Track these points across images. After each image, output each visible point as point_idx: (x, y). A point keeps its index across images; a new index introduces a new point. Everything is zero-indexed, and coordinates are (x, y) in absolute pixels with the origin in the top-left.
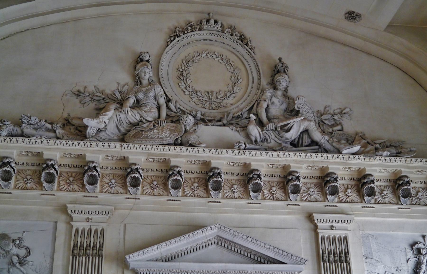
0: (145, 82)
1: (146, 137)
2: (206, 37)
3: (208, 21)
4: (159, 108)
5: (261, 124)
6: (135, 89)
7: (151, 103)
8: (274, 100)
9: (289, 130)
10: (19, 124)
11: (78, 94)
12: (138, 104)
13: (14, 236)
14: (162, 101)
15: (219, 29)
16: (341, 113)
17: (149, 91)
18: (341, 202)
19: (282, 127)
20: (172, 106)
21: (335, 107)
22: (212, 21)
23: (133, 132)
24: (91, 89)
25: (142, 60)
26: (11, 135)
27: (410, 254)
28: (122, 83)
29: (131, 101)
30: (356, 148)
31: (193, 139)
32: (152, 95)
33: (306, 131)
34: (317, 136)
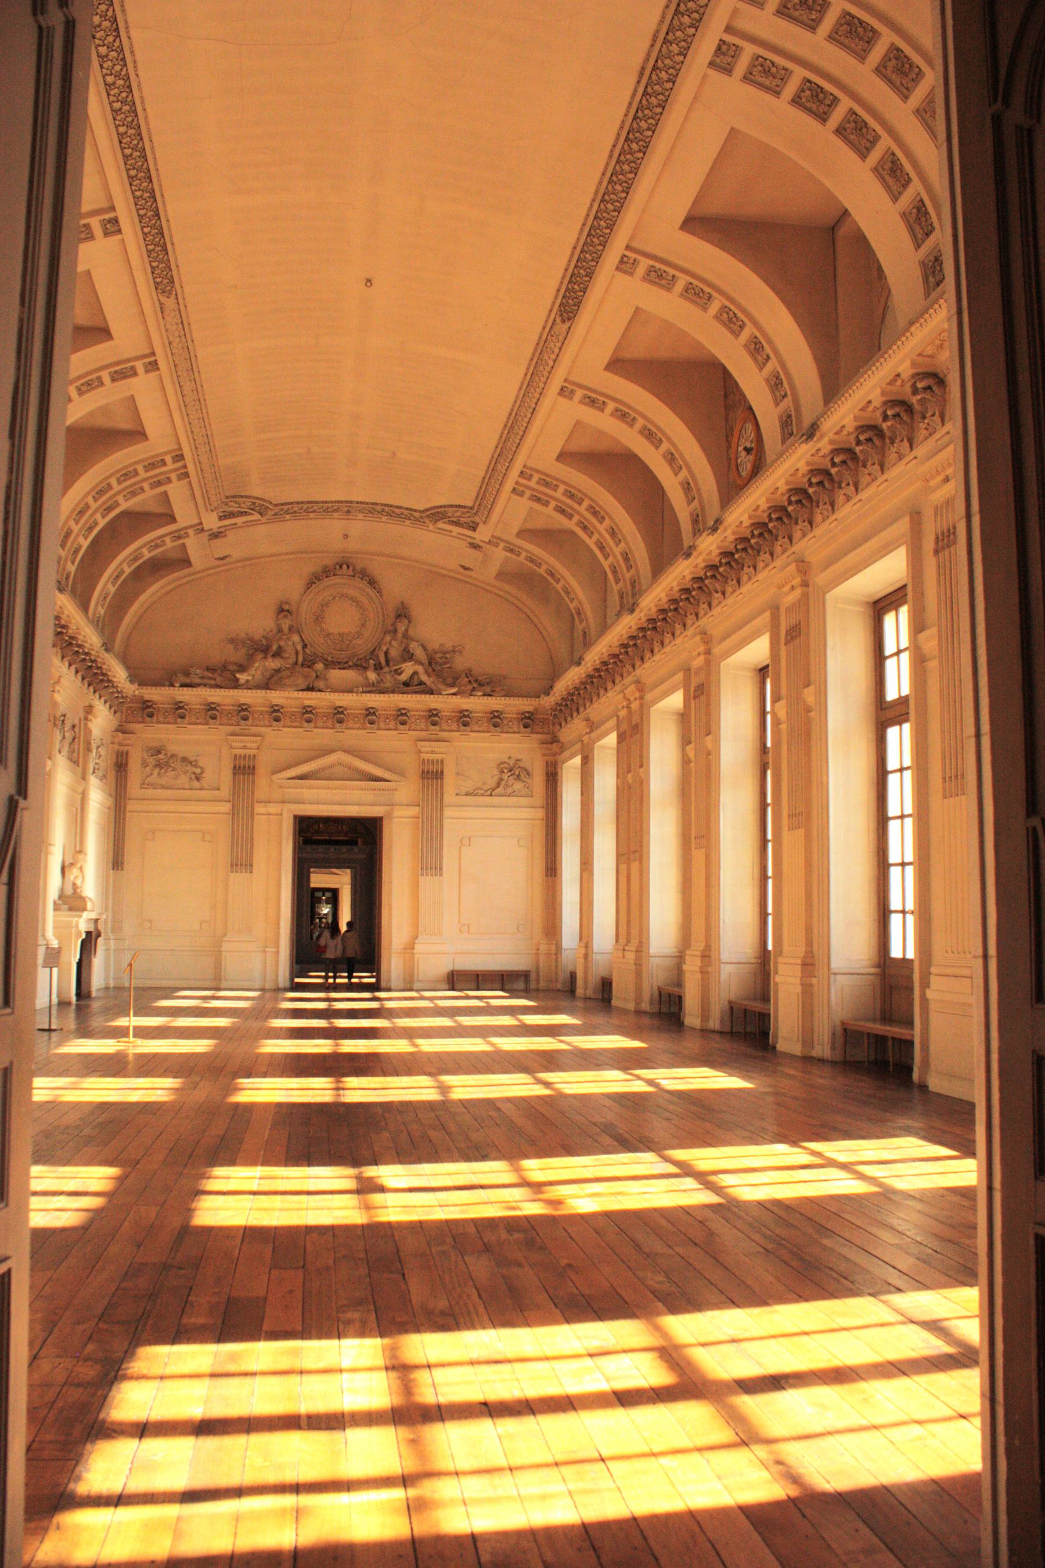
0: (286, 629)
1: (285, 685)
2: (339, 581)
3: (341, 567)
4: (297, 653)
5: (378, 668)
6: (278, 637)
7: (289, 653)
8: (394, 643)
9: (400, 674)
10: (187, 674)
11: (232, 641)
12: (278, 654)
13: (192, 759)
14: (299, 647)
15: (351, 573)
16: (454, 651)
17: (289, 639)
18: (442, 731)
19: (396, 671)
20: (307, 651)
21: (449, 646)
22: (345, 567)
23: (276, 678)
24: (243, 635)
25: (283, 610)
26: (183, 685)
27: (496, 772)
28: (268, 630)
29: (275, 647)
30: (454, 690)
31: (320, 684)
32: (290, 643)
33: (415, 673)
34: (424, 678)
